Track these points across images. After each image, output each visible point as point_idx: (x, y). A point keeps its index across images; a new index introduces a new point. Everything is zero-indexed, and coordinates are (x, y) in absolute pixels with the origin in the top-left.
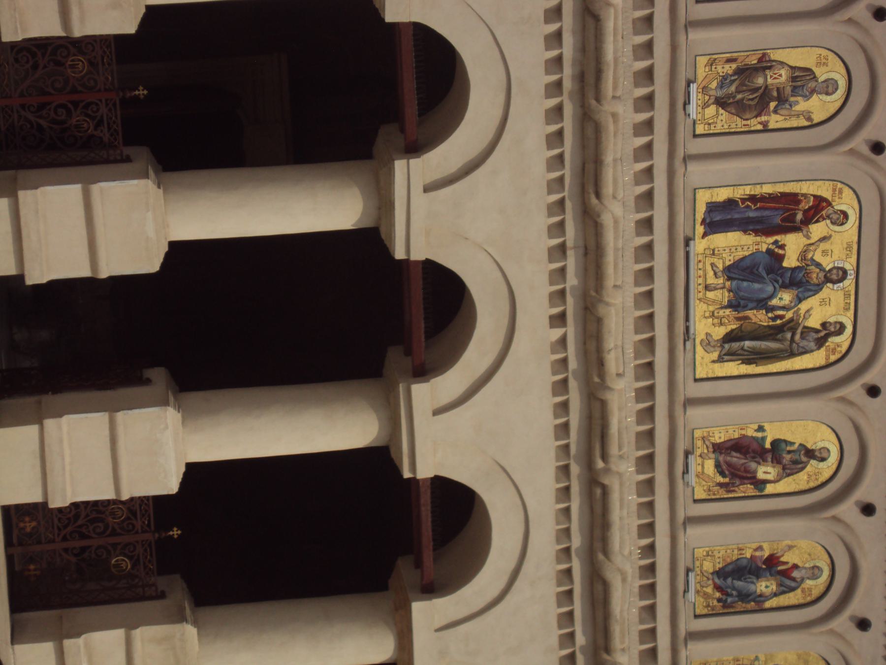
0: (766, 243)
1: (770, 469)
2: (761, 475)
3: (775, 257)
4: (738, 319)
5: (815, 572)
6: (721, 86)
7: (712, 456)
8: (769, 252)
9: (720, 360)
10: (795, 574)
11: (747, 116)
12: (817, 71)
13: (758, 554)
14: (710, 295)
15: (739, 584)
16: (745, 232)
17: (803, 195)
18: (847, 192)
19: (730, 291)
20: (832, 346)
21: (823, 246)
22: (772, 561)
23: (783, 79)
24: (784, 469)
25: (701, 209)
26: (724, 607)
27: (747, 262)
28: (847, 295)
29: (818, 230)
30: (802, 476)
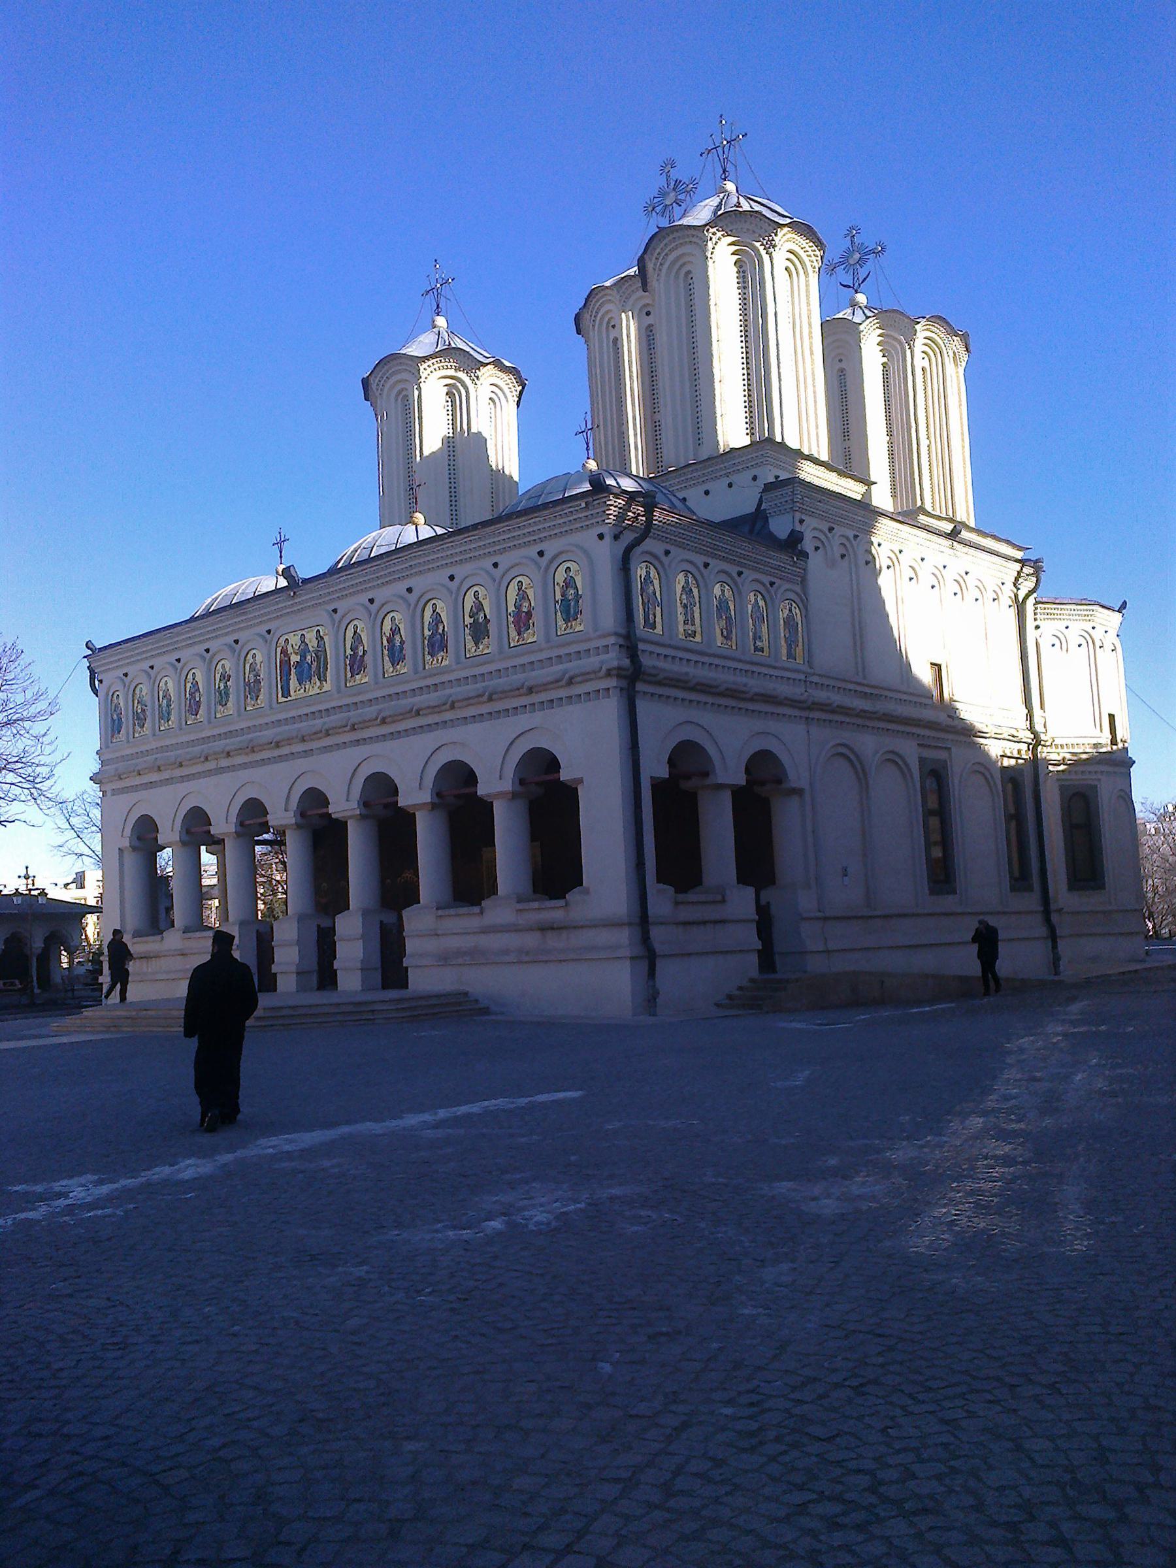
0: (293, 671)
9: (326, 681)
28: (308, 632)
29: (290, 650)
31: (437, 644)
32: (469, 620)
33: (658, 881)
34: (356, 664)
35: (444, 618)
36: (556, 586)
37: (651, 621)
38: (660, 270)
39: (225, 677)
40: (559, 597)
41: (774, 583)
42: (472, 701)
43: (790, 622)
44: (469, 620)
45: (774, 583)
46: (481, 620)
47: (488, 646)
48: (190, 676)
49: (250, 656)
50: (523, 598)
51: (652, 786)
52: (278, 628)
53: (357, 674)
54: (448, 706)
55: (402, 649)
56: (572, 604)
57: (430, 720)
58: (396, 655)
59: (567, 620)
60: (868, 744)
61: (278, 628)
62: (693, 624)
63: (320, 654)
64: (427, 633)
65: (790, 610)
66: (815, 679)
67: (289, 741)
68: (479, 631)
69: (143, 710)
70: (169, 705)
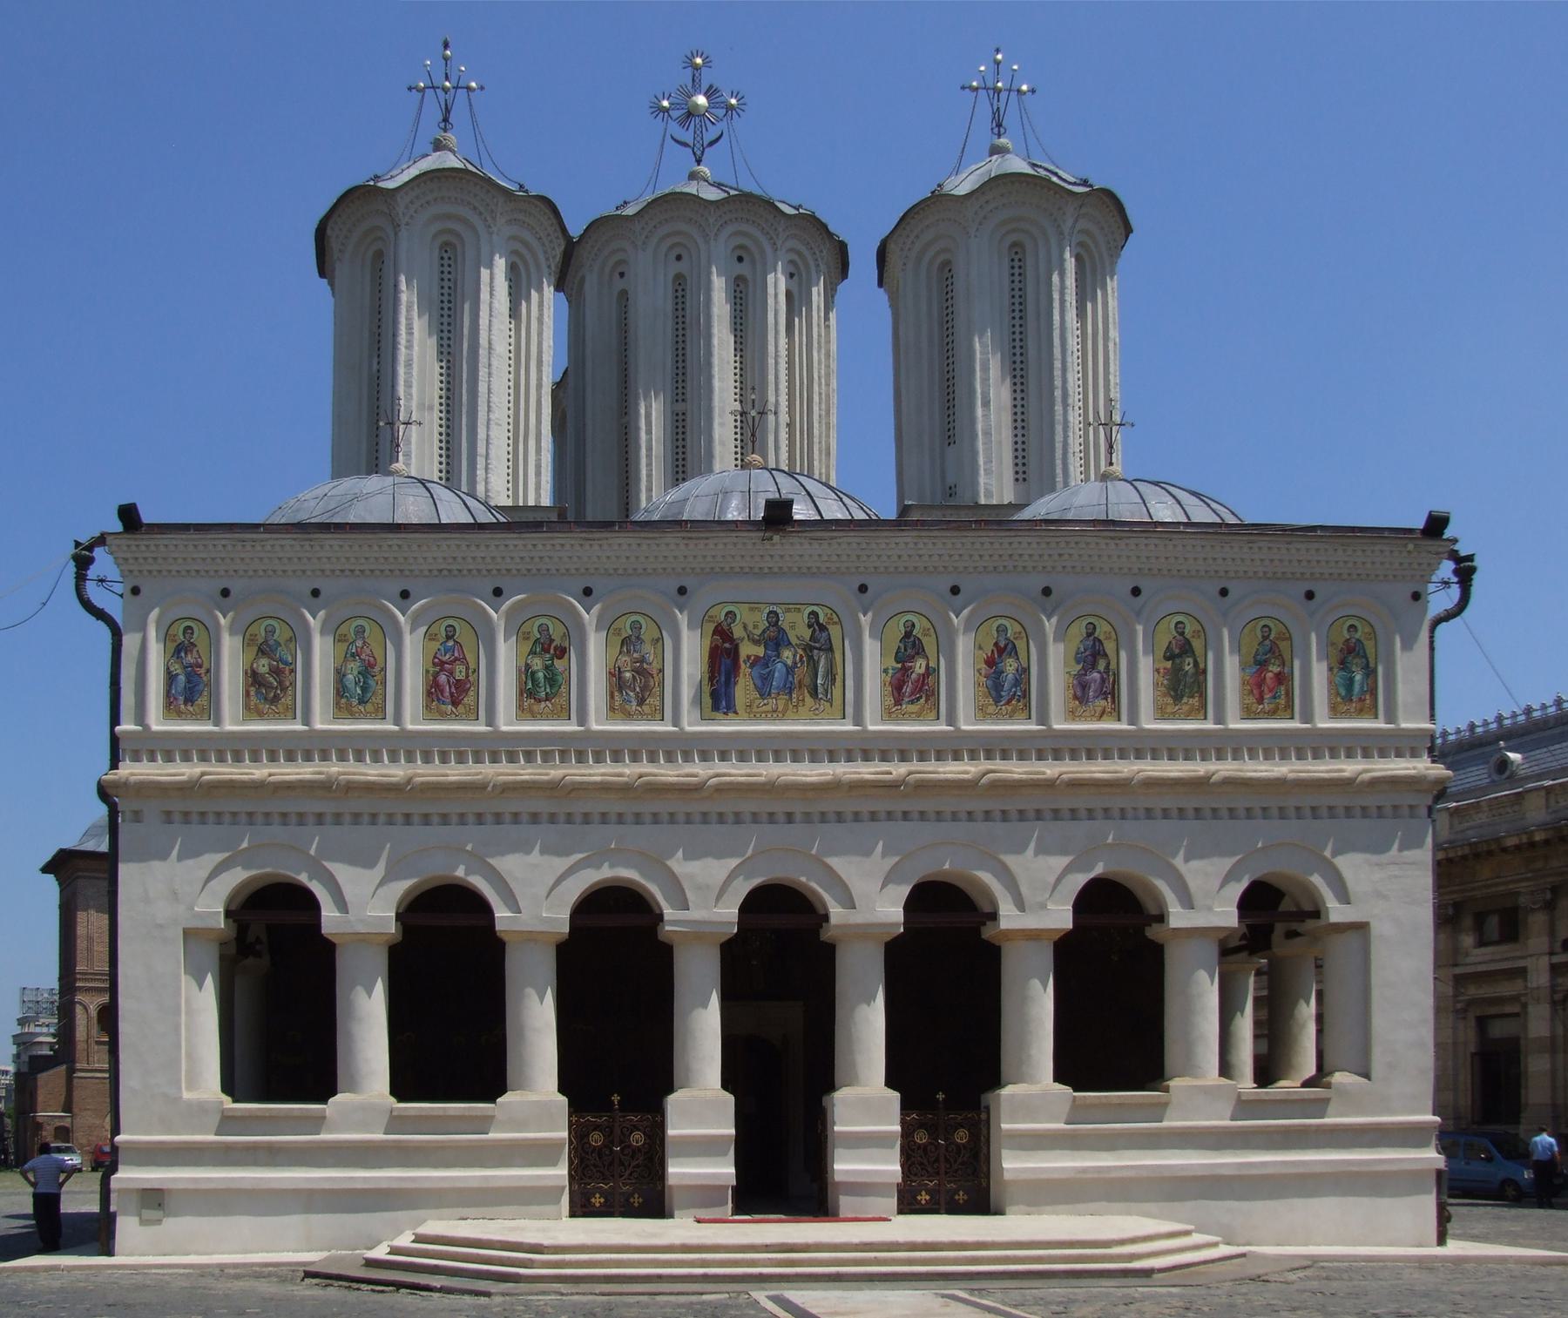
0: (744, 668)
1: (918, 665)
2: (923, 670)
3: (755, 662)
4: (800, 687)
5: (1002, 630)
7: (904, 706)
8: (752, 666)
9: (830, 701)
10: (1002, 644)
11: (652, 683)
12: (624, 635)
13: (983, 672)
14: (780, 708)
15: (1006, 686)
16: (736, 683)
17: (711, 643)
18: (713, 612)
19: (779, 694)
20: (826, 620)
21: (750, 628)
22: (990, 662)
23: (627, 658)
24: (918, 654)
26: (1024, 697)
27: (759, 683)
28: (788, 610)
29: (738, 632)
30: (925, 640)
53: (908, 702)
69: (275, 672)
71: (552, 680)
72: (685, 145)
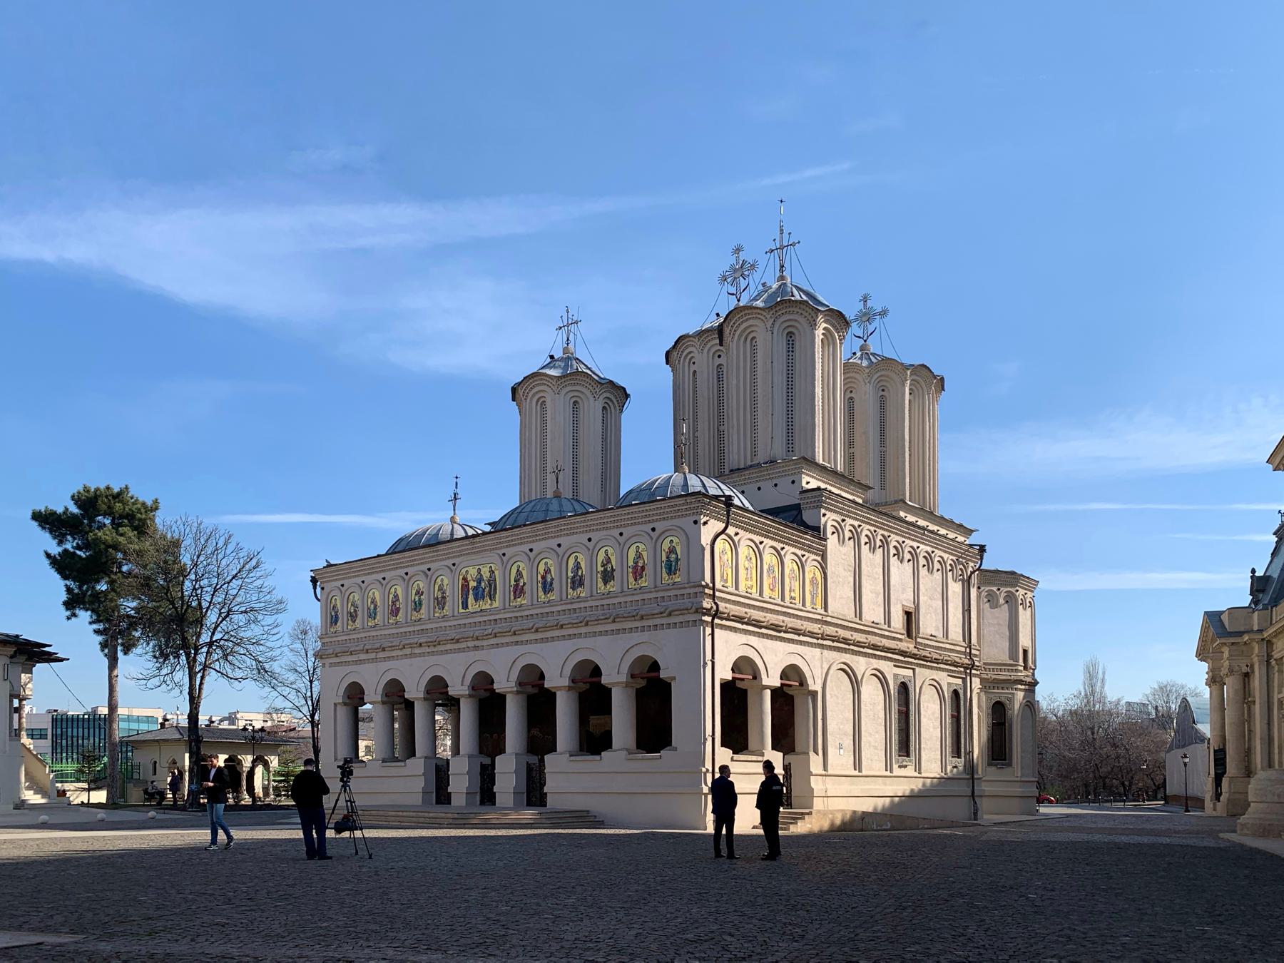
0: (471, 592)
3: (475, 588)
6: (440, 609)
22: (543, 577)
25: (464, 611)
29: (469, 578)
31: (577, 582)
32: (600, 569)
33: (722, 746)
34: (518, 591)
35: (583, 565)
36: (663, 552)
37: (725, 578)
38: (734, 334)
39: (419, 593)
40: (664, 558)
41: (804, 555)
42: (600, 622)
43: (813, 581)
44: (600, 569)
45: (804, 555)
46: (609, 569)
47: (613, 587)
48: (393, 590)
49: (439, 580)
50: (639, 557)
51: (721, 684)
52: (461, 563)
54: (583, 624)
55: (551, 584)
56: (674, 564)
57: (571, 631)
58: (547, 587)
59: (669, 573)
60: (862, 665)
61: (461, 563)
62: (752, 581)
63: (492, 583)
64: (570, 574)
65: (814, 573)
66: (829, 619)
67: (466, 639)
68: (607, 576)
69: (355, 611)
70: (375, 608)
71: (420, 604)
72: (733, 294)
